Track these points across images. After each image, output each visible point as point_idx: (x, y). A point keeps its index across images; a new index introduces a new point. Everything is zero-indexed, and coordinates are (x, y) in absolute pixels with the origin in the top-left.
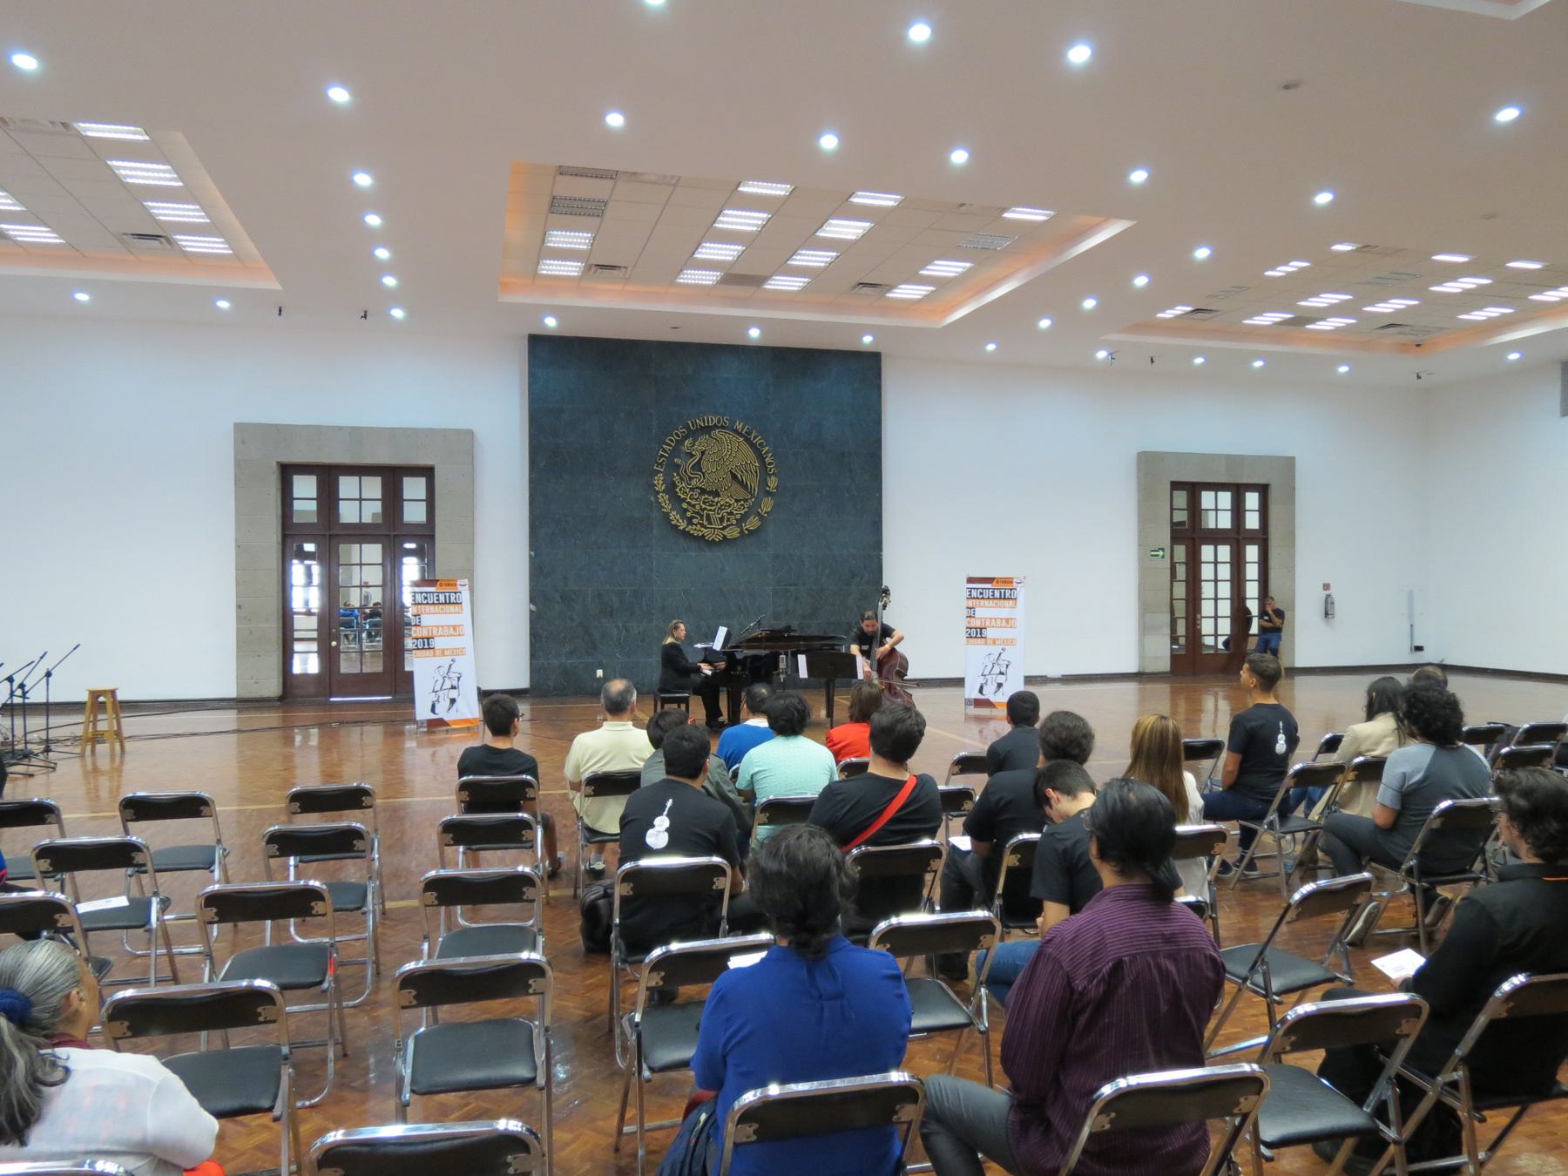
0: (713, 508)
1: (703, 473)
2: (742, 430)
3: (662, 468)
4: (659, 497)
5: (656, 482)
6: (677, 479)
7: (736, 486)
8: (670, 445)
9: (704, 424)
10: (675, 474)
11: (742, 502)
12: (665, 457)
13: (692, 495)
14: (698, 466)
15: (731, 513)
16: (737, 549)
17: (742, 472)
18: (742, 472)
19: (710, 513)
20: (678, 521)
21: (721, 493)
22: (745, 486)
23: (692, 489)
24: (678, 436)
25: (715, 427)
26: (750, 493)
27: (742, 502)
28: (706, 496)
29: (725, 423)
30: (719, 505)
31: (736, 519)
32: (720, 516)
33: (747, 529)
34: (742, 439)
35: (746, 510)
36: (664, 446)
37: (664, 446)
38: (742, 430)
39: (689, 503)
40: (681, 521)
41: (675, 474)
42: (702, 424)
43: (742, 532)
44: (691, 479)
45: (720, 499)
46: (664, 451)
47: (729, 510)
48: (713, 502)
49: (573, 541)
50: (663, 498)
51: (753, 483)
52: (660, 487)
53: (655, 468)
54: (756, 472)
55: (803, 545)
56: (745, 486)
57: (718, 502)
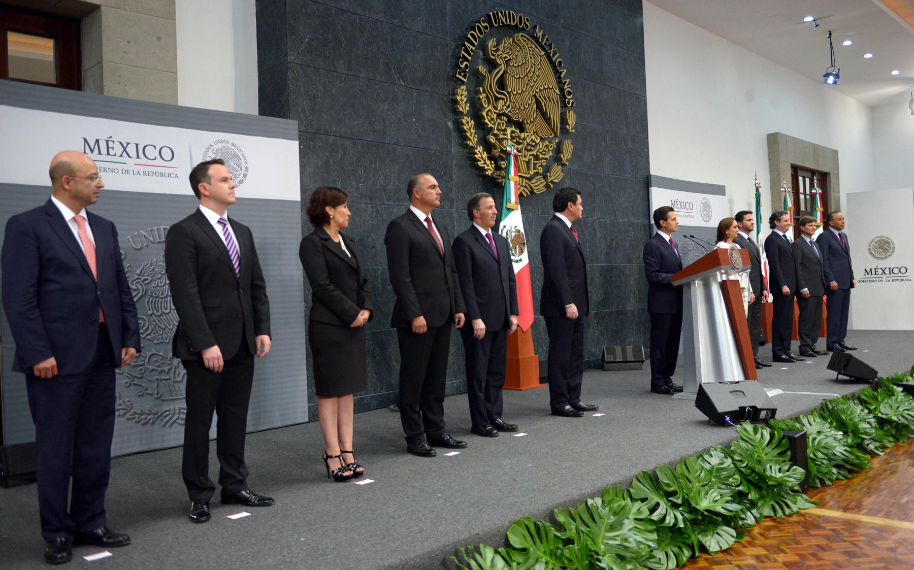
0: (520, 147)
1: (508, 93)
2: (542, 40)
3: (465, 76)
4: (464, 121)
5: (458, 98)
6: (482, 96)
7: (540, 118)
8: (474, 45)
9: (506, 21)
10: (481, 89)
11: (547, 143)
12: (467, 60)
13: (499, 123)
14: (502, 84)
15: (536, 157)
16: (538, 211)
17: (546, 100)
18: (546, 100)
19: (519, 154)
20: (485, 163)
21: (527, 126)
22: (548, 120)
23: (499, 115)
24: (481, 33)
25: (516, 29)
26: (553, 130)
27: (547, 143)
28: (513, 129)
29: (527, 26)
30: (525, 144)
31: (541, 166)
32: (527, 160)
33: (551, 182)
34: (543, 53)
35: (551, 154)
36: (466, 44)
37: (466, 44)
38: (542, 40)
39: (496, 135)
40: (488, 162)
41: (481, 89)
42: (504, 21)
43: (547, 186)
44: (497, 99)
45: (526, 134)
46: (466, 50)
47: (534, 153)
48: (519, 137)
49: (354, 184)
50: (468, 124)
51: (555, 117)
52: (464, 107)
53: (458, 76)
54: (557, 102)
55: (594, 208)
56: (548, 120)
57: (524, 139)
